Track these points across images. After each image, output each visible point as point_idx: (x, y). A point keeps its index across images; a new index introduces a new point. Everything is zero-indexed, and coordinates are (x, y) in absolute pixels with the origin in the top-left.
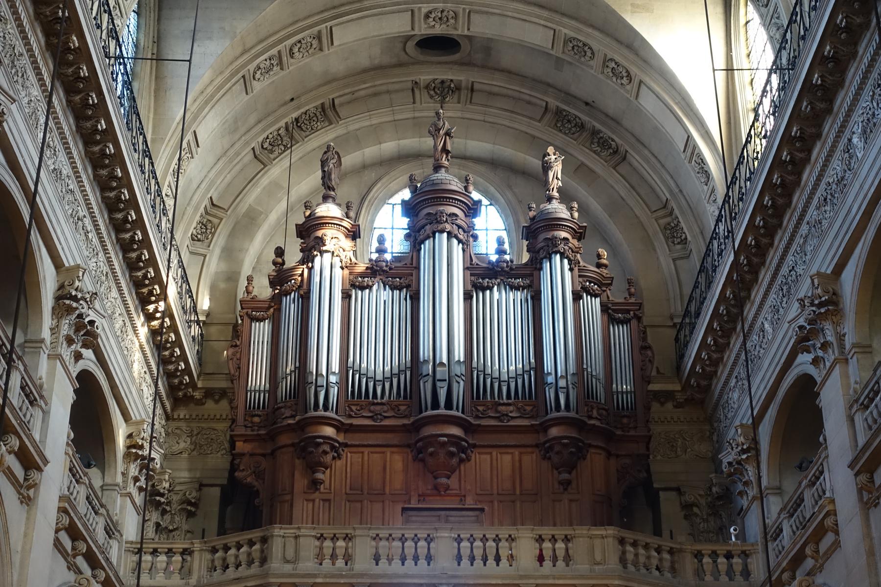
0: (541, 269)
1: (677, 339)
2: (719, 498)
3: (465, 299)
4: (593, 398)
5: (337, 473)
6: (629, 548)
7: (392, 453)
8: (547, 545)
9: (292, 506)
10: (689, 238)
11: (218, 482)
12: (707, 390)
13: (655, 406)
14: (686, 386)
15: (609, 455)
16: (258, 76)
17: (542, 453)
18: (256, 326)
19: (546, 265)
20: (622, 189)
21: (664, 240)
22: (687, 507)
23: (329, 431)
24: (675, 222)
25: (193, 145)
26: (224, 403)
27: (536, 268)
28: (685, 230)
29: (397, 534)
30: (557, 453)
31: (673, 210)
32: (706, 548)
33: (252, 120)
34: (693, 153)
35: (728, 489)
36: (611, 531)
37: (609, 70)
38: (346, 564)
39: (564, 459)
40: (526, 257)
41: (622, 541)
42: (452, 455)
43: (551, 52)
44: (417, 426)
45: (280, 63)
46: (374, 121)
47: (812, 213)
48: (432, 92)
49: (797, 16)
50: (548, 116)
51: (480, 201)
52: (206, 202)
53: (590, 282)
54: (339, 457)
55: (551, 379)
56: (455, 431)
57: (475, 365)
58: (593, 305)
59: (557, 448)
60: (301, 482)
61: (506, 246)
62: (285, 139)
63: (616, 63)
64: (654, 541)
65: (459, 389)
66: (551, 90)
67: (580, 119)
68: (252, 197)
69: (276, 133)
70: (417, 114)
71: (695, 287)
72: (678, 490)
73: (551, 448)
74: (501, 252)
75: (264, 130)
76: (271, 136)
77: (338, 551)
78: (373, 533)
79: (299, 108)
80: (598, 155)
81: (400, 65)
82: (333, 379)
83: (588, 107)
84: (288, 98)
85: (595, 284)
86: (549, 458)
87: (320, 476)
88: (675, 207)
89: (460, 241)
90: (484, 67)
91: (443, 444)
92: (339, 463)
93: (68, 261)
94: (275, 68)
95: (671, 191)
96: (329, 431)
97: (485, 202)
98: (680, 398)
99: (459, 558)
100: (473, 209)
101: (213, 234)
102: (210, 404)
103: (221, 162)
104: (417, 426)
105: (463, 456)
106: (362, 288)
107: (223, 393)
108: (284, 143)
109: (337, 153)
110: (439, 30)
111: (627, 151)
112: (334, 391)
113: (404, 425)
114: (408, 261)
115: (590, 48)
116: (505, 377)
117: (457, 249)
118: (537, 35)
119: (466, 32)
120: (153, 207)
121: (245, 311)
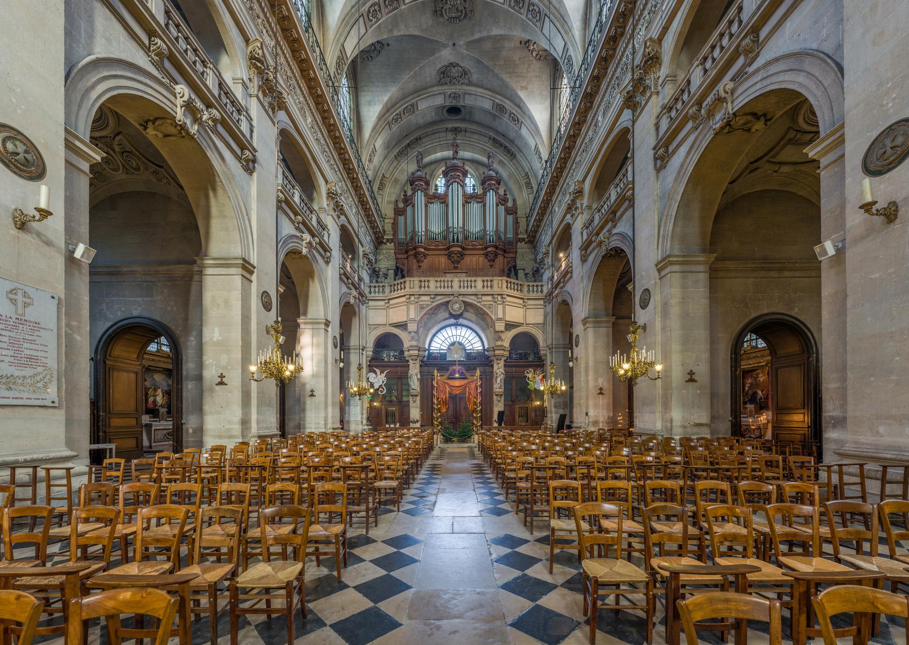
5: (426, 263)
23: (423, 250)
32: (531, 284)
33: (394, 143)
36: (505, 278)
39: (491, 258)
44: (449, 248)
56: (459, 249)
60: (415, 266)
64: (516, 282)
65: (461, 237)
74: (474, 189)
81: (441, 121)
96: (423, 250)
104: (449, 248)
110: (454, 103)
112: (423, 238)
118: (487, 105)
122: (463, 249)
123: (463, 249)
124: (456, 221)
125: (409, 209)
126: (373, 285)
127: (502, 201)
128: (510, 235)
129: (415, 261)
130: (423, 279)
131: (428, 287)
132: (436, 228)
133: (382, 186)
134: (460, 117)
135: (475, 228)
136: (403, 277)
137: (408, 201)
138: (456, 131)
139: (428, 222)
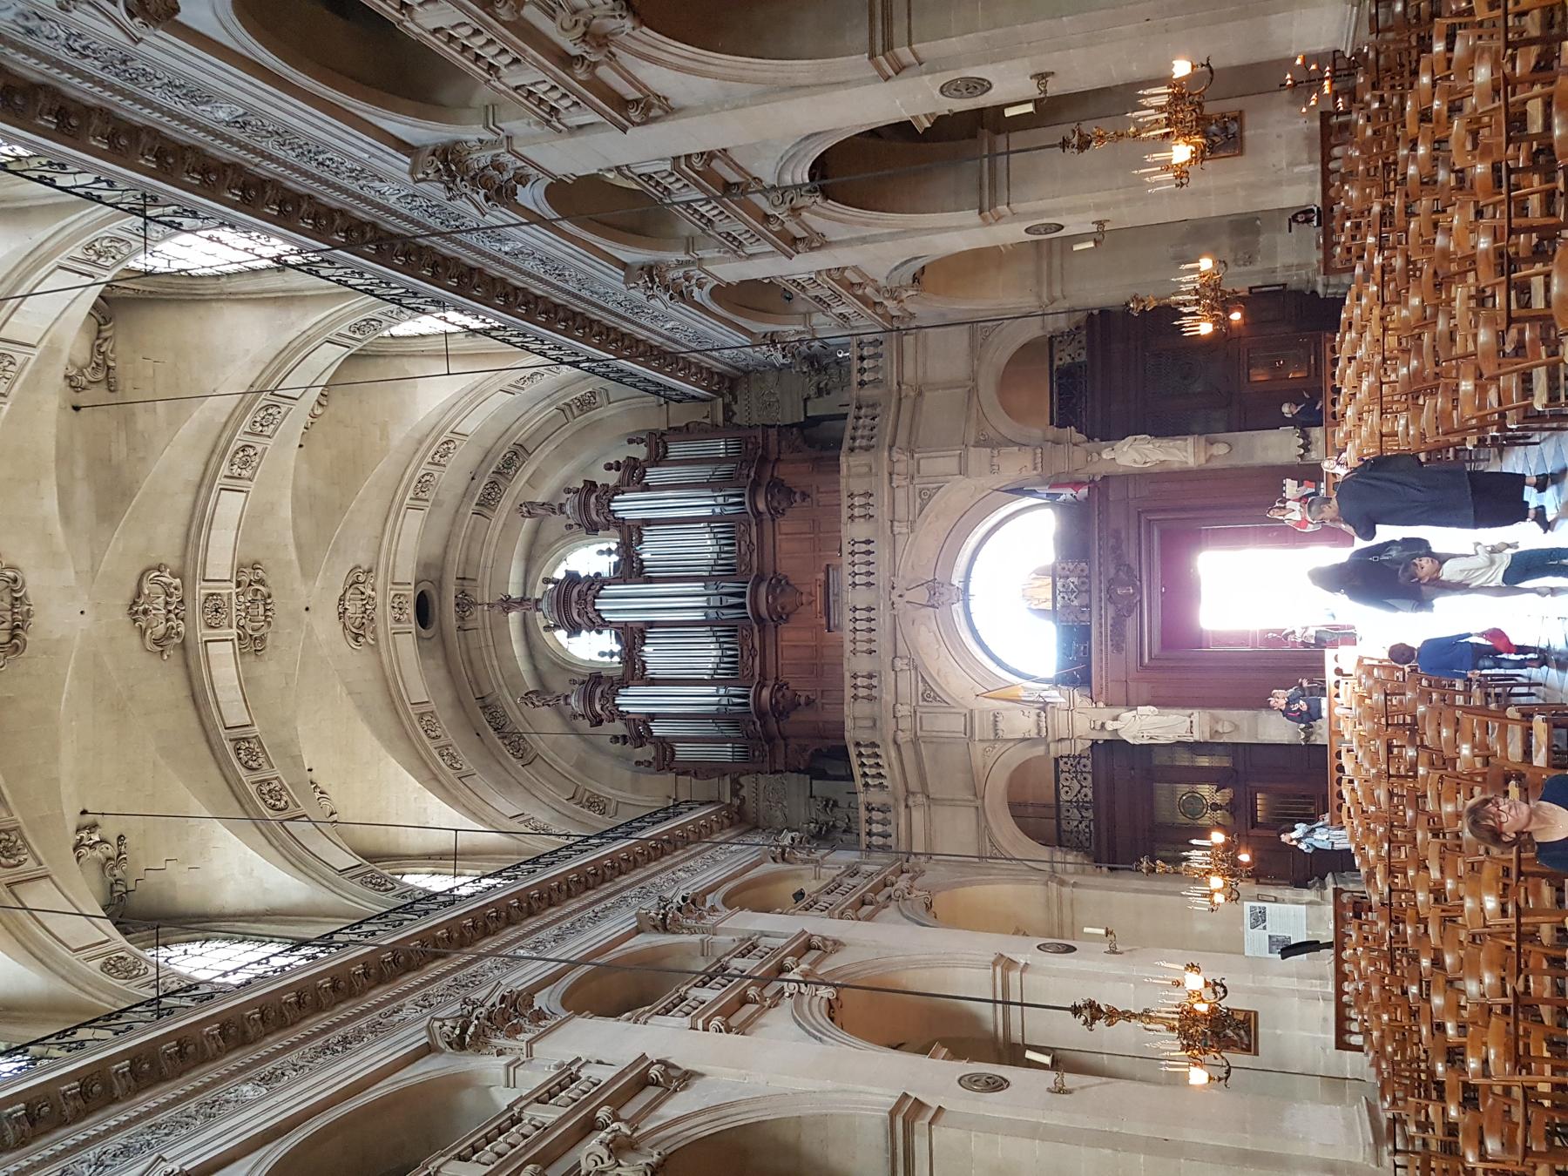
1: (679, 401)
2: (812, 364)
5: (801, 687)
6: (857, 443)
8: (857, 512)
13: (735, 420)
14: (719, 393)
15: (778, 460)
18: (678, 757)
19: (619, 515)
20: (549, 448)
22: (820, 392)
23: (766, 693)
26: (742, 780)
32: (856, 378)
33: (498, 768)
39: (783, 492)
40: (613, 531)
41: (852, 450)
45: (446, 747)
47: (572, 286)
50: (485, 511)
52: (571, 803)
55: (718, 510)
56: (763, 589)
58: (653, 475)
61: (604, 547)
64: (850, 421)
65: (730, 587)
68: (564, 765)
72: (805, 400)
73: (776, 509)
74: (609, 552)
81: (443, 641)
82: (722, 691)
87: (802, 700)
90: (442, 569)
91: (775, 599)
93: (632, 924)
95: (550, 405)
96: (766, 693)
98: (728, 398)
99: (869, 584)
100: (572, 578)
102: (743, 792)
104: (760, 619)
106: (645, 669)
107: (735, 781)
110: (411, 610)
112: (732, 690)
116: (717, 549)
117: (610, 590)
122: (760, 579)
123: (760, 579)
124: (683, 602)
125: (658, 730)
127: (633, 475)
128: (720, 447)
129: (793, 717)
130: (849, 692)
132: (705, 655)
133: (596, 803)
134: (434, 592)
135: (701, 547)
136: (843, 753)
137: (639, 730)
138: (465, 603)
139: (686, 677)
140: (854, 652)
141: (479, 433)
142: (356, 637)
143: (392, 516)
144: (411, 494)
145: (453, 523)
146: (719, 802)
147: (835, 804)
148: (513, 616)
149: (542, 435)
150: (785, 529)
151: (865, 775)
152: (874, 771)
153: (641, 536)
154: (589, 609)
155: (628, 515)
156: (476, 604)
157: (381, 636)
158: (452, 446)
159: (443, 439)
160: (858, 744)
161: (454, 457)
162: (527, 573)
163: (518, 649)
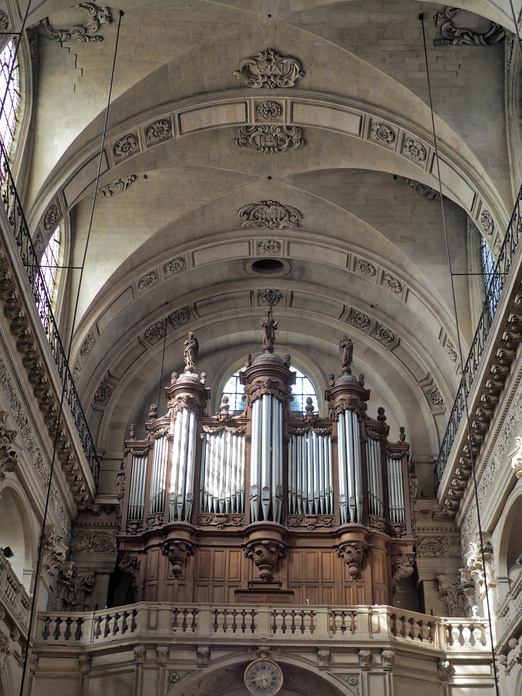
0: (338, 421)
3: (283, 442)
4: (374, 513)
7: (230, 551)
9: (157, 588)
10: (444, 400)
11: (108, 571)
12: (456, 509)
16: (141, 286)
17: (337, 552)
18: (137, 461)
19: (341, 417)
20: (396, 366)
21: (426, 402)
24: (435, 389)
25: (95, 333)
27: (334, 420)
28: (441, 394)
29: (230, 609)
30: (349, 552)
31: (432, 380)
34: (445, 340)
35: (472, 580)
37: (387, 282)
38: (193, 631)
42: (272, 553)
43: (347, 270)
46: (223, 319)
48: (264, 299)
49: (509, 236)
51: (295, 373)
52: (105, 373)
53: (373, 431)
54: (192, 554)
56: (276, 536)
57: (290, 489)
59: (348, 549)
61: (315, 404)
62: (161, 330)
63: (391, 277)
66: (347, 297)
67: (367, 317)
68: (136, 370)
69: (154, 326)
70: (254, 314)
71: (447, 433)
73: (344, 549)
74: (310, 408)
75: (146, 324)
76: (151, 329)
77: (187, 621)
78: (213, 609)
79: (171, 309)
80: (380, 342)
81: (242, 279)
83: (373, 309)
84: (163, 302)
85: (376, 432)
86: (343, 556)
88: (434, 378)
89: (280, 401)
91: (265, 546)
92: (192, 558)
94: (154, 281)
95: (431, 367)
97: (299, 374)
99: (275, 628)
101: (109, 396)
103: (116, 346)
105: (281, 554)
108: (160, 333)
109: (196, 339)
110: (267, 255)
111: (400, 339)
113: (239, 532)
114: (244, 414)
115: (373, 267)
119: (286, 257)
120: (61, 373)
121: (128, 449)
126: (54, 616)
127: (373, 431)
129: (163, 559)
131: (194, 625)
134: (281, 274)
140: (216, 612)
141: (407, 311)
142: (247, 213)
143: (342, 243)
144: (359, 257)
145: (336, 290)
146: (97, 494)
147: (88, 594)
148: (262, 334)
149: (407, 362)
150: (326, 556)
151: (109, 618)
152: (111, 626)
153: (323, 435)
154: (263, 391)
155: (340, 425)
156: (271, 306)
157: (247, 232)
158: (398, 290)
159: (403, 282)
160: (135, 613)
161: (389, 290)
162: (295, 346)
163: (234, 336)
